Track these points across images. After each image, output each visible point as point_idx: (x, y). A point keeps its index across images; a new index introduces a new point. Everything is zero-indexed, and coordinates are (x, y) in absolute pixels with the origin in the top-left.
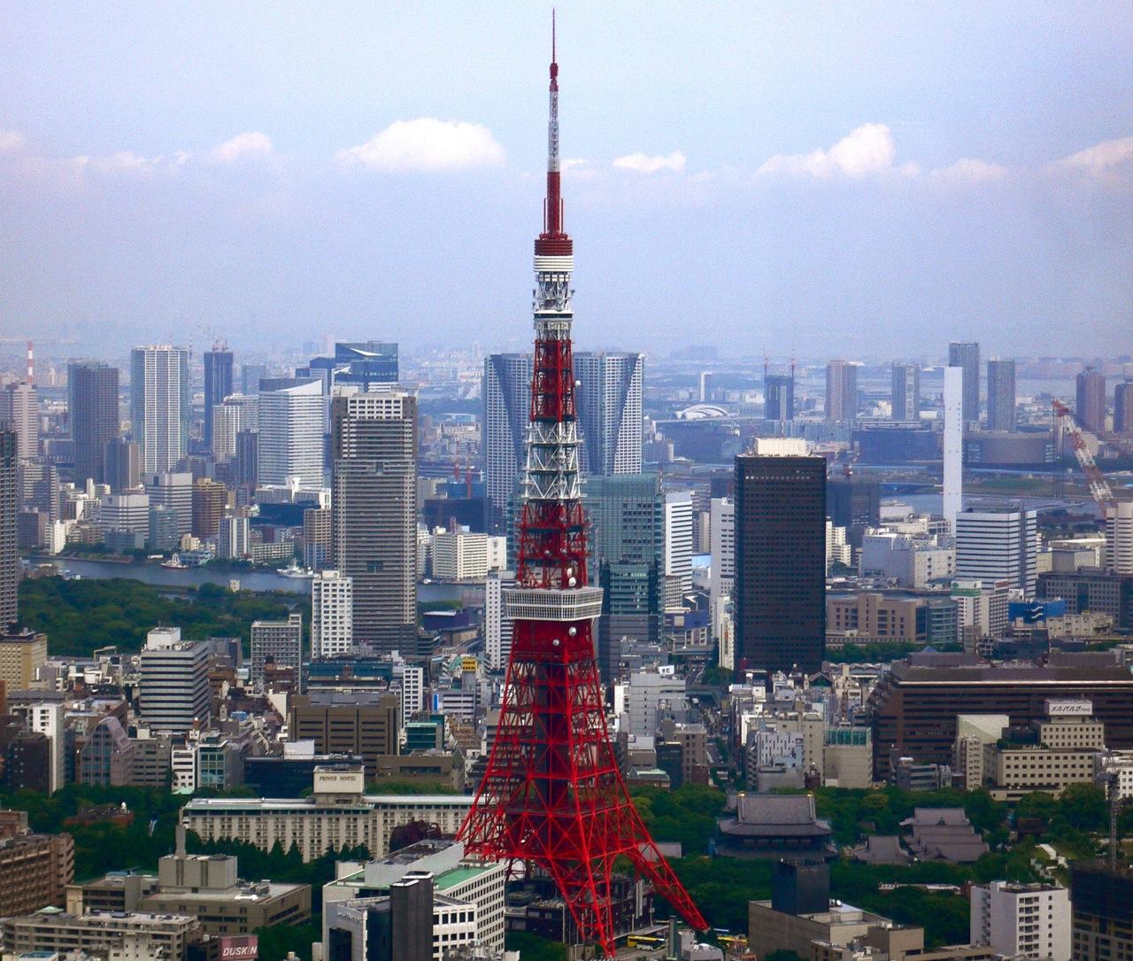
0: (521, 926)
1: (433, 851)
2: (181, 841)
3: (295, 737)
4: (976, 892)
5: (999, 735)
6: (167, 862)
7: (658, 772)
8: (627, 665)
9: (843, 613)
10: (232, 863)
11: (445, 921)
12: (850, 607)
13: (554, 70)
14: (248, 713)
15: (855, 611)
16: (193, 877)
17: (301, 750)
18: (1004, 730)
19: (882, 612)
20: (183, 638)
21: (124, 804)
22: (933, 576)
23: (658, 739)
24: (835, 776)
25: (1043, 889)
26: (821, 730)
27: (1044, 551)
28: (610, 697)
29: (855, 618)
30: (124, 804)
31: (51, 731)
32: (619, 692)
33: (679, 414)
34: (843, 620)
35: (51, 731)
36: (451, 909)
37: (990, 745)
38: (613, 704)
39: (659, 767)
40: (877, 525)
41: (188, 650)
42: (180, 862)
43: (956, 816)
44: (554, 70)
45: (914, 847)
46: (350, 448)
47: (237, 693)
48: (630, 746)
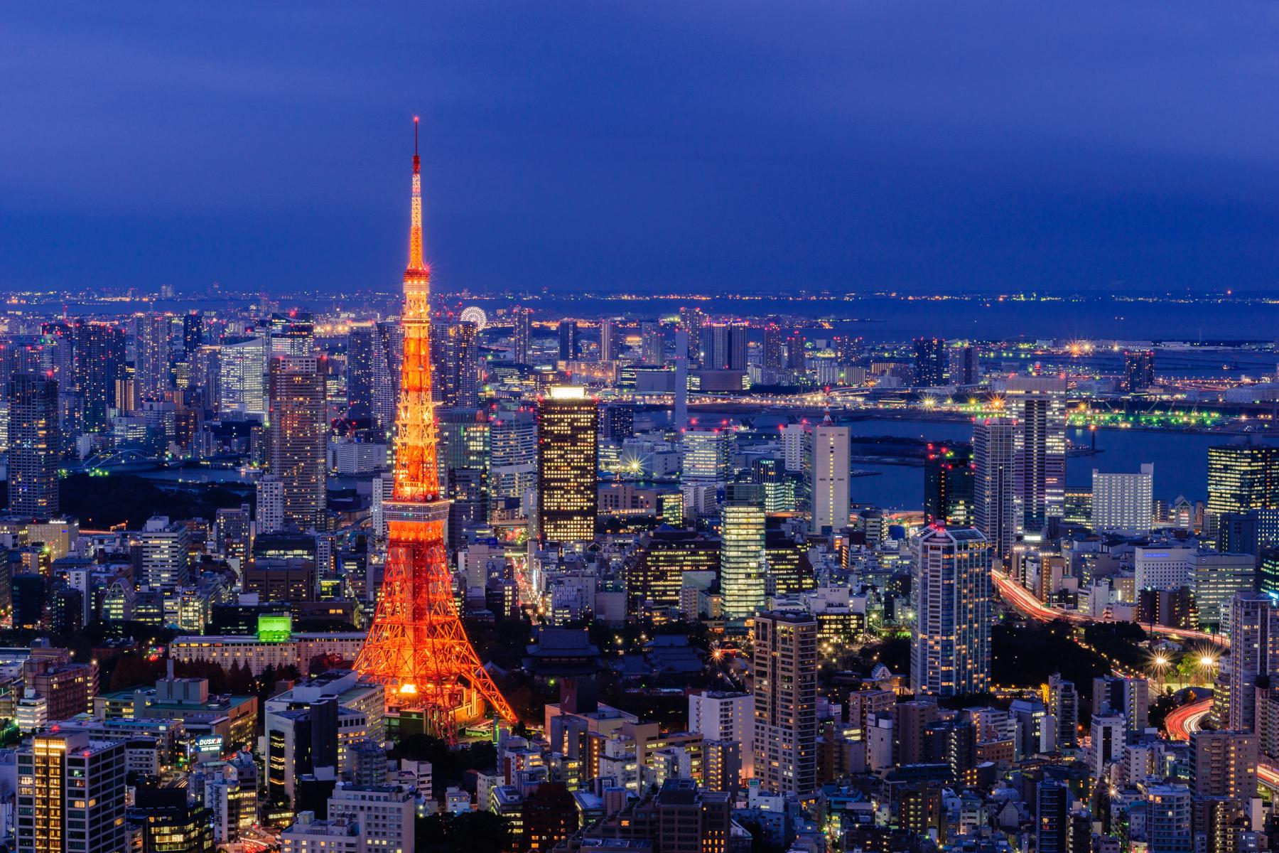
0: (395, 723)
1: (338, 677)
2: (170, 666)
3: (247, 590)
4: (692, 698)
5: (709, 585)
6: (161, 685)
7: (486, 611)
8: (467, 537)
9: (609, 499)
10: (205, 684)
11: (346, 725)
12: (614, 494)
13: (416, 161)
14: (214, 572)
15: (617, 497)
16: (178, 693)
17: (252, 600)
18: (713, 581)
19: (633, 497)
20: (171, 522)
21: (132, 638)
22: (668, 471)
23: (487, 590)
24: (602, 612)
25: (735, 696)
26: (591, 582)
27: (740, 454)
28: (455, 560)
29: (617, 501)
30: (132, 638)
31: (83, 587)
32: (461, 556)
33: (502, 355)
34: (608, 502)
35: (83, 587)
36: (349, 717)
37: (703, 591)
38: (457, 563)
39: (488, 608)
40: (631, 435)
41: (174, 532)
42: (170, 684)
43: (681, 640)
44: (416, 161)
45: (654, 662)
46: (281, 385)
47: (206, 559)
48: (469, 594)
